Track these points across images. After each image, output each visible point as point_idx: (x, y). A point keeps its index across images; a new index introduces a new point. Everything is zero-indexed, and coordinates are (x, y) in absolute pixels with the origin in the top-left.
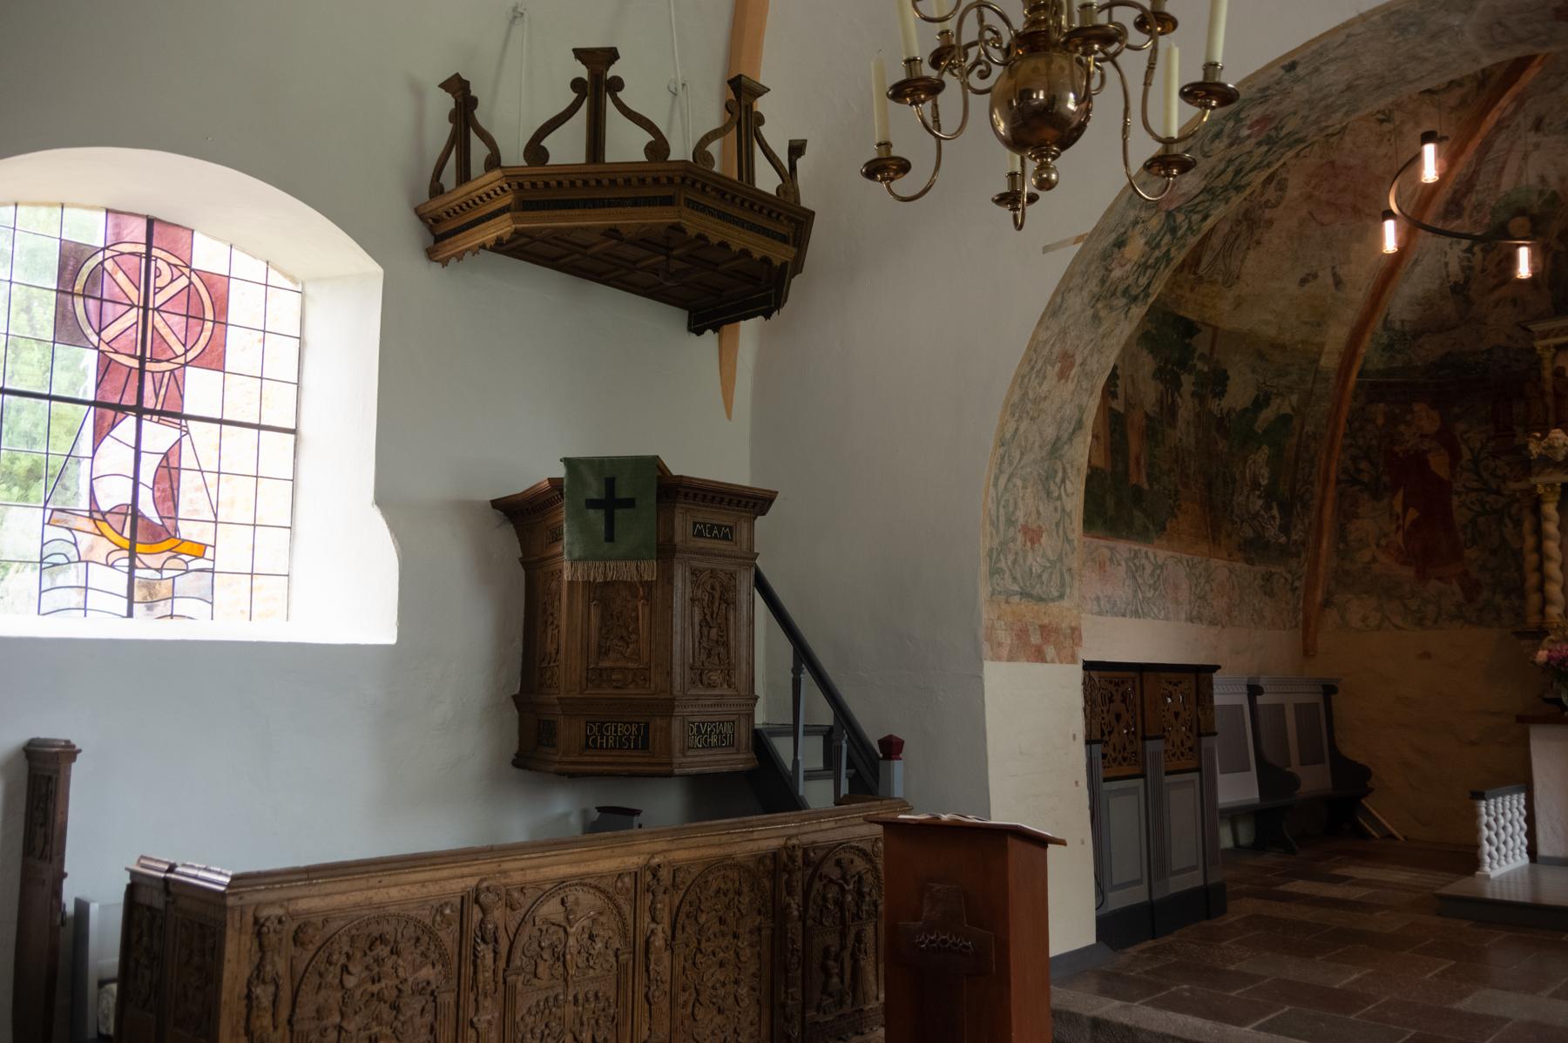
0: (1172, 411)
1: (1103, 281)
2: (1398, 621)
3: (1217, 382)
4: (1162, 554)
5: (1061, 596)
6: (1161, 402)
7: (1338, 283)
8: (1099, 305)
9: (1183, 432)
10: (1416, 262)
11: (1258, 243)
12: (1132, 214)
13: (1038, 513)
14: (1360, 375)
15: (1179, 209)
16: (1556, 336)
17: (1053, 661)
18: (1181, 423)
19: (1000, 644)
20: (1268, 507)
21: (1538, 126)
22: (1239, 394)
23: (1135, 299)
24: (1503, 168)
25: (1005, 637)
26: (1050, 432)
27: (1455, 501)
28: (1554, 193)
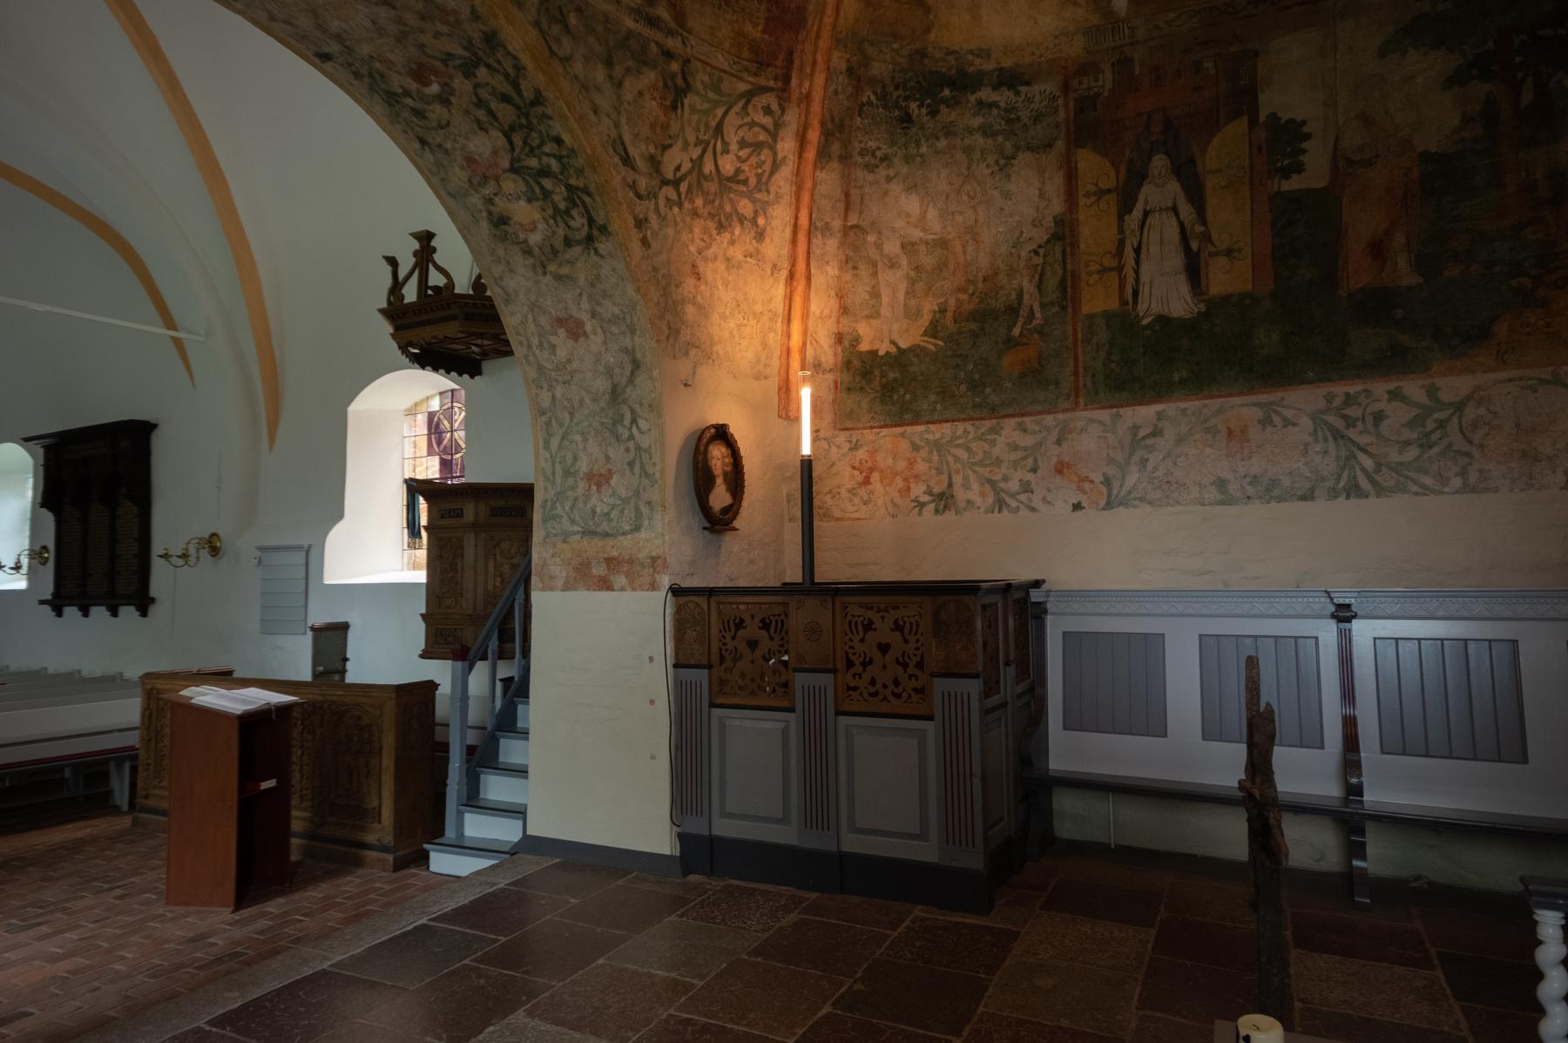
1: (528, 252)
4: (1454, 386)
5: (637, 529)
8: (552, 268)
12: (475, 200)
13: (607, 458)
15: (512, 161)
17: (623, 589)
23: (590, 239)
25: (559, 572)
26: (601, 384)
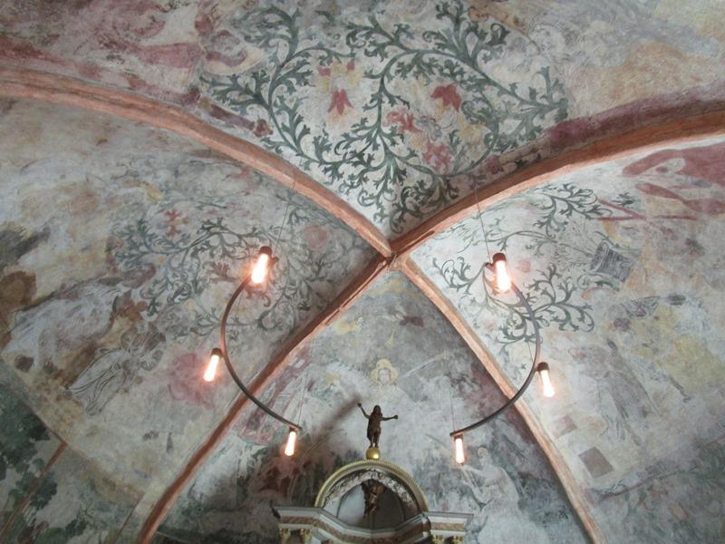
3: (43, 491)
7: (170, 447)
10: (223, 451)
11: (126, 391)
14: (160, 529)
16: (293, 523)
21: (310, 387)
22: (57, 513)
24: (286, 407)
28: (308, 435)
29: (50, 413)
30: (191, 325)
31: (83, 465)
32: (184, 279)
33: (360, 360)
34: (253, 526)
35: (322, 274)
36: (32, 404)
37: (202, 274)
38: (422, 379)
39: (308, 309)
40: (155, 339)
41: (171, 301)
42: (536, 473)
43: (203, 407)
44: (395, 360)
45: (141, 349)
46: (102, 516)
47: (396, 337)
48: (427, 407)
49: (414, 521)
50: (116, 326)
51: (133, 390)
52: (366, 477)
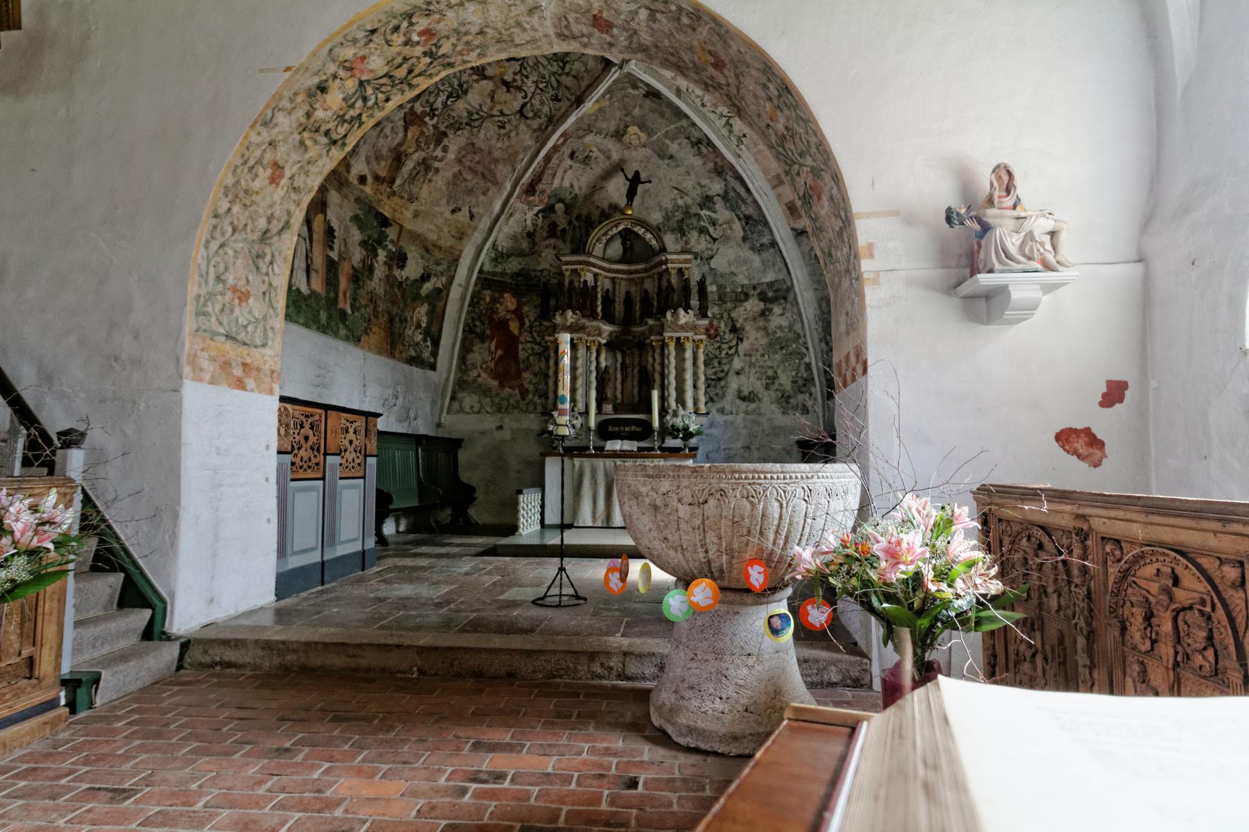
0: (371, 269)
2: (488, 409)
3: (400, 259)
5: (264, 345)
6: (363, 261)
7: (472, 217)
8: (306, 135)
9: (376, 283)
12: (332, 68)
13: (247, 280)
14: (480, 271)
15: (368, 81)
17: (252, 391)
18: (376, 278)
19: (201, 370)
20: (425, 340)
21: (572, 156)
22: (412, 270)
23: (335, 142)
26: (262, 223)
27: (520, 346)
29: (387, 208)
30: (465, 121)
31: (417, 238)
32: (451, 85)
33: (612, 125)
34: (544, 265)
35: (567, 70)
36: (375, 205)
37: (465, 78)
38: (667, 142)
39: (559, 100)
40: (440, 137)
41: (445, 104)
42: (756, 217)
43: (489, 184)
44: (642, 126)
45: (432, 146)
46: (440, 268)
47: (641, 107)
48: (673, 164)
49: (657, 259)
50: (410, 134)
51: (435, 178)
52: (621, 227)
